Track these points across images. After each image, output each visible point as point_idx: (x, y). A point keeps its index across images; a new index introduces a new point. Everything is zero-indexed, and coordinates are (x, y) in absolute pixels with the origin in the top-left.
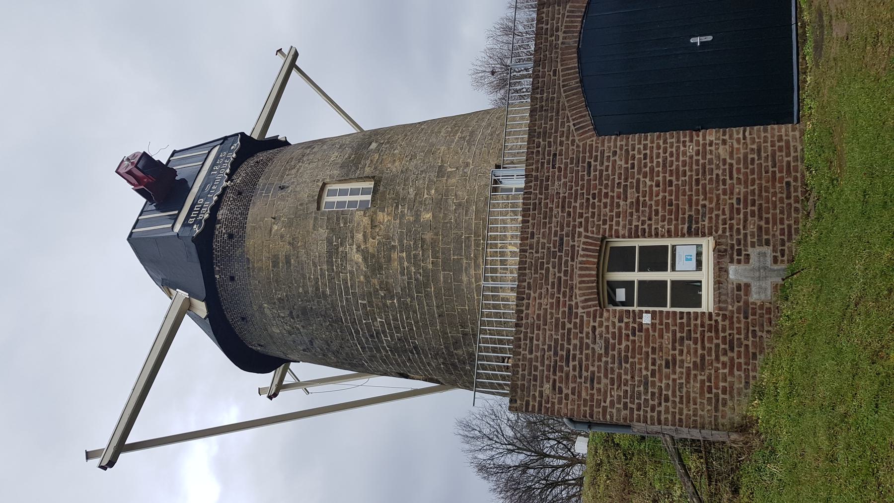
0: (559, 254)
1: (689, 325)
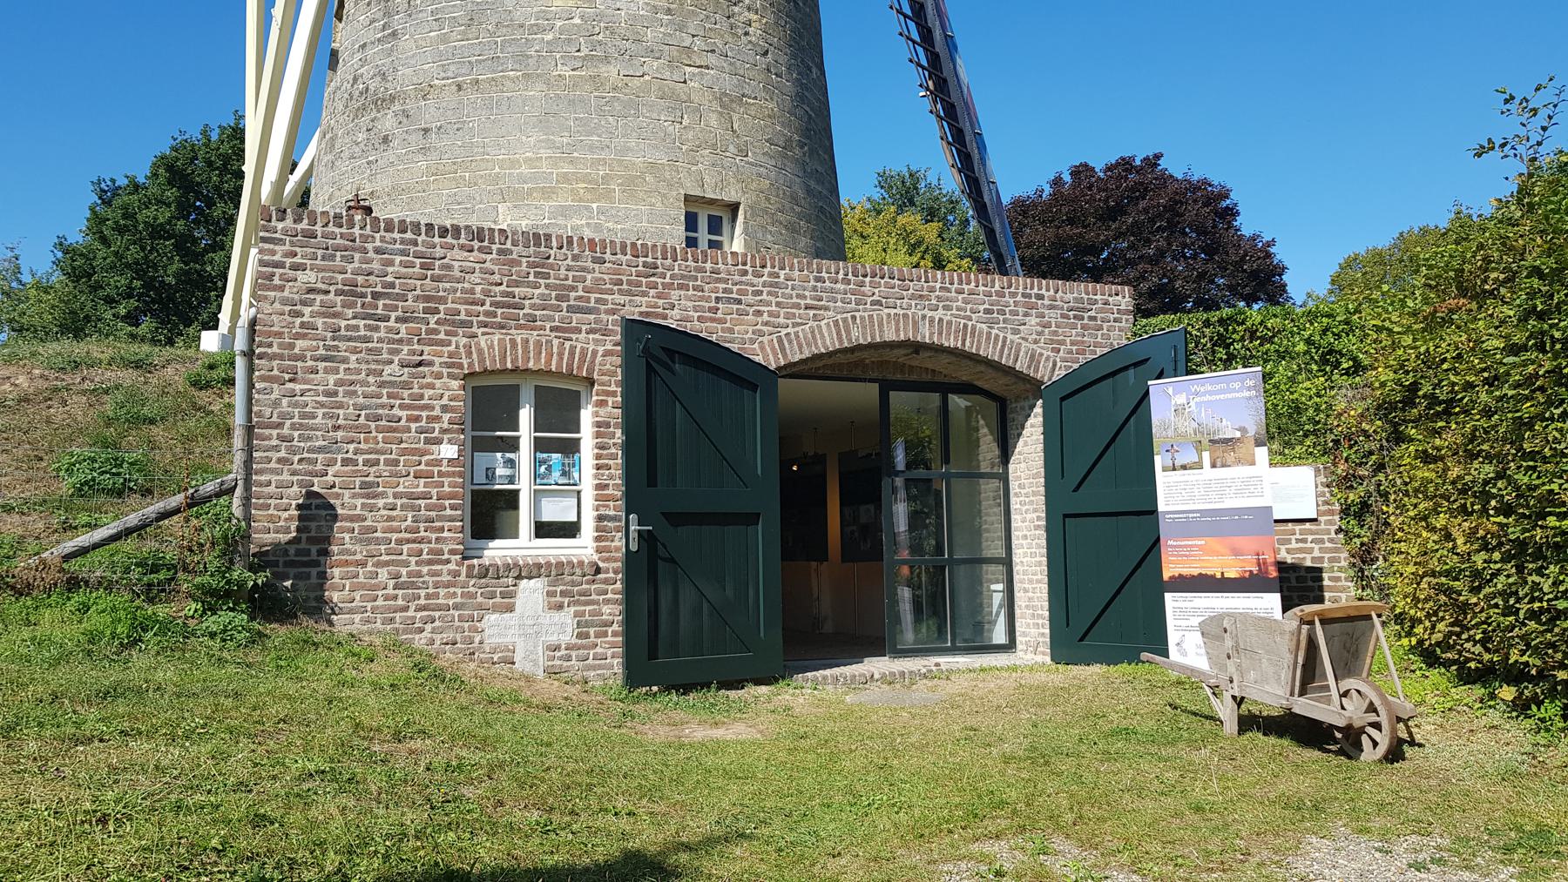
0: (565, 305)
1: (440, 518)
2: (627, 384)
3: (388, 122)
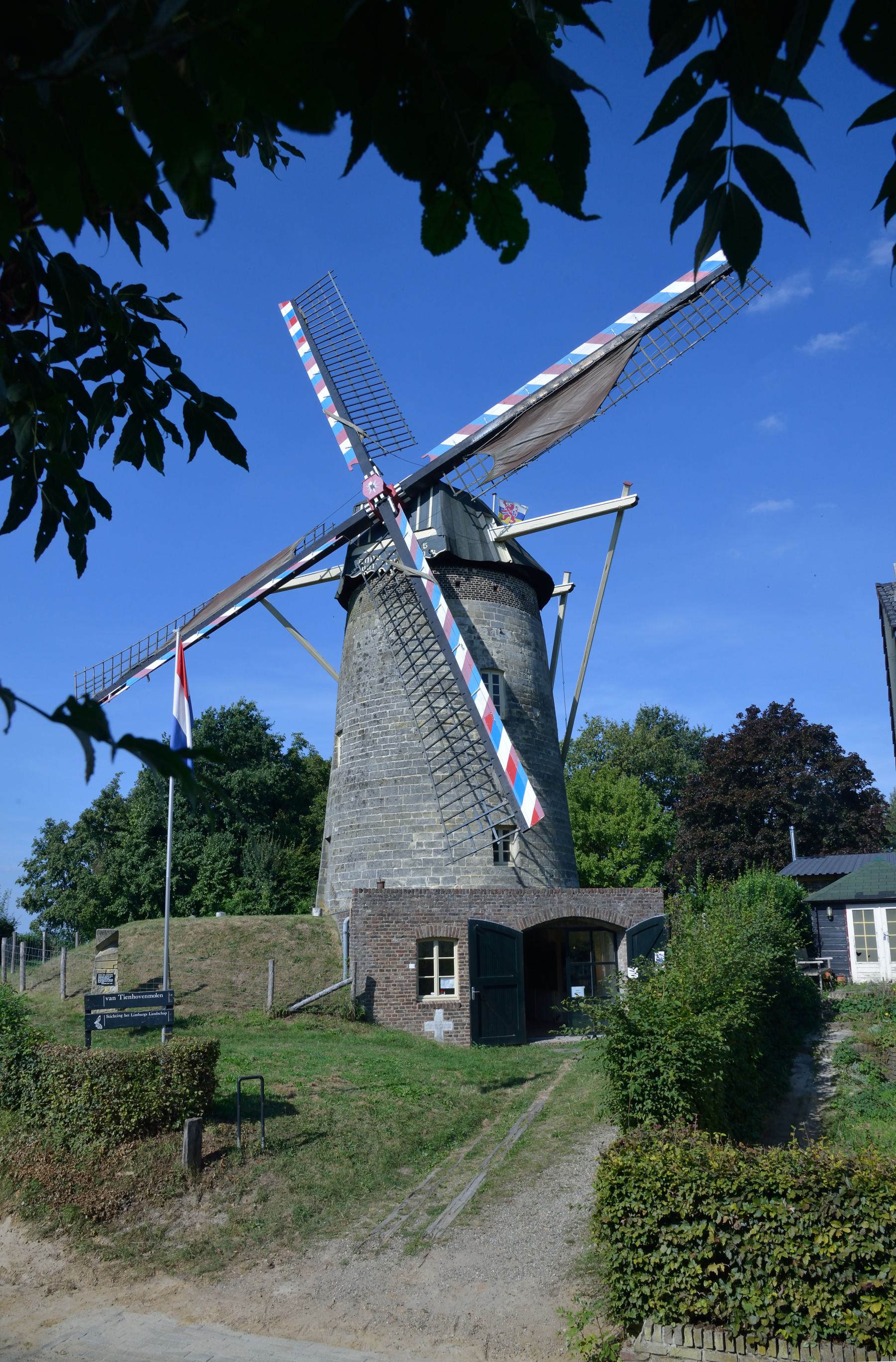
2: (470, 940)
3: (365, 795)
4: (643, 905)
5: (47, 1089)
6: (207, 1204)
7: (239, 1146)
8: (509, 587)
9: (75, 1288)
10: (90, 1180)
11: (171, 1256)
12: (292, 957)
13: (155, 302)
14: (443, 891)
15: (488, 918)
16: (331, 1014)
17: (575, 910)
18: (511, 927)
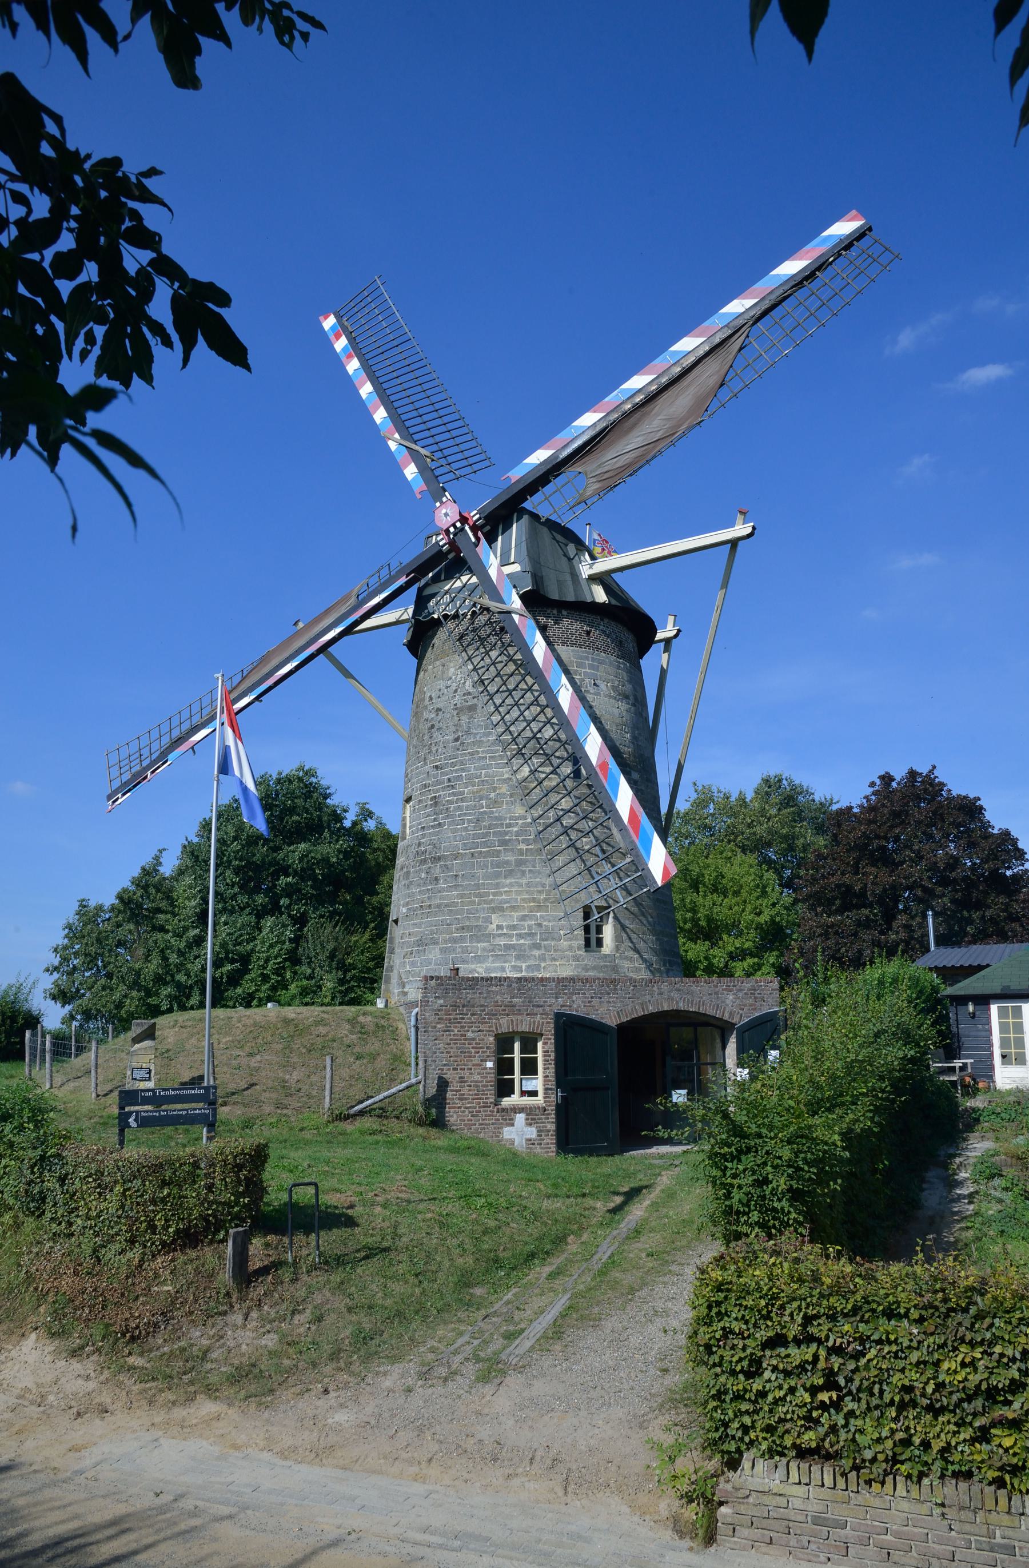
3: (437, 871)
4: (755, 998)
5: (74, 1194)
6: (254, 1324)
7: (290, 1260)
8: (604, 632)
9: (107, 1412)
10: (123, 1295)
11: (213, 1379)
12: (353, 1054)
13: (133, 179)
14: (526, 979)
15: (577, 1011)
16: (398, 1118)
17: (677, 1002)
18: (604, 1021)
